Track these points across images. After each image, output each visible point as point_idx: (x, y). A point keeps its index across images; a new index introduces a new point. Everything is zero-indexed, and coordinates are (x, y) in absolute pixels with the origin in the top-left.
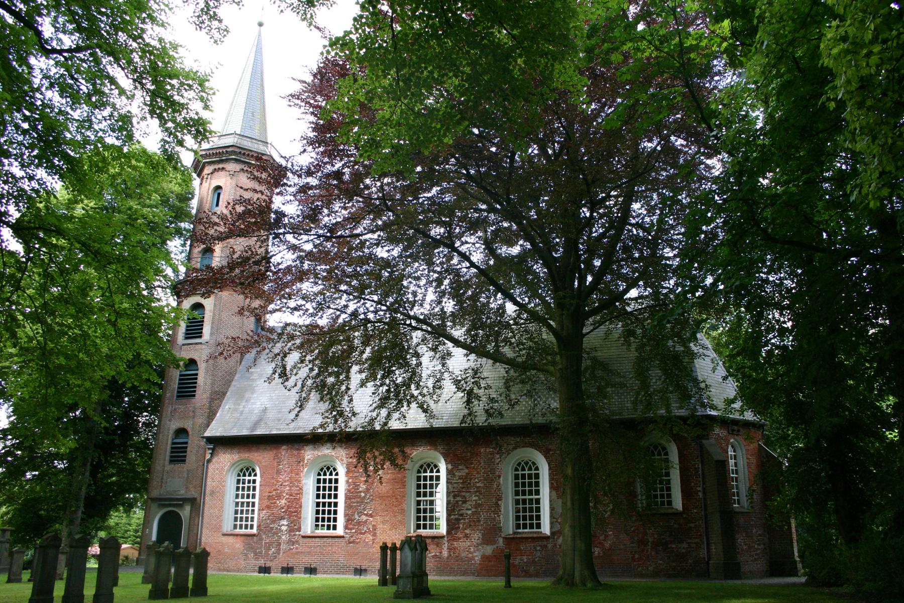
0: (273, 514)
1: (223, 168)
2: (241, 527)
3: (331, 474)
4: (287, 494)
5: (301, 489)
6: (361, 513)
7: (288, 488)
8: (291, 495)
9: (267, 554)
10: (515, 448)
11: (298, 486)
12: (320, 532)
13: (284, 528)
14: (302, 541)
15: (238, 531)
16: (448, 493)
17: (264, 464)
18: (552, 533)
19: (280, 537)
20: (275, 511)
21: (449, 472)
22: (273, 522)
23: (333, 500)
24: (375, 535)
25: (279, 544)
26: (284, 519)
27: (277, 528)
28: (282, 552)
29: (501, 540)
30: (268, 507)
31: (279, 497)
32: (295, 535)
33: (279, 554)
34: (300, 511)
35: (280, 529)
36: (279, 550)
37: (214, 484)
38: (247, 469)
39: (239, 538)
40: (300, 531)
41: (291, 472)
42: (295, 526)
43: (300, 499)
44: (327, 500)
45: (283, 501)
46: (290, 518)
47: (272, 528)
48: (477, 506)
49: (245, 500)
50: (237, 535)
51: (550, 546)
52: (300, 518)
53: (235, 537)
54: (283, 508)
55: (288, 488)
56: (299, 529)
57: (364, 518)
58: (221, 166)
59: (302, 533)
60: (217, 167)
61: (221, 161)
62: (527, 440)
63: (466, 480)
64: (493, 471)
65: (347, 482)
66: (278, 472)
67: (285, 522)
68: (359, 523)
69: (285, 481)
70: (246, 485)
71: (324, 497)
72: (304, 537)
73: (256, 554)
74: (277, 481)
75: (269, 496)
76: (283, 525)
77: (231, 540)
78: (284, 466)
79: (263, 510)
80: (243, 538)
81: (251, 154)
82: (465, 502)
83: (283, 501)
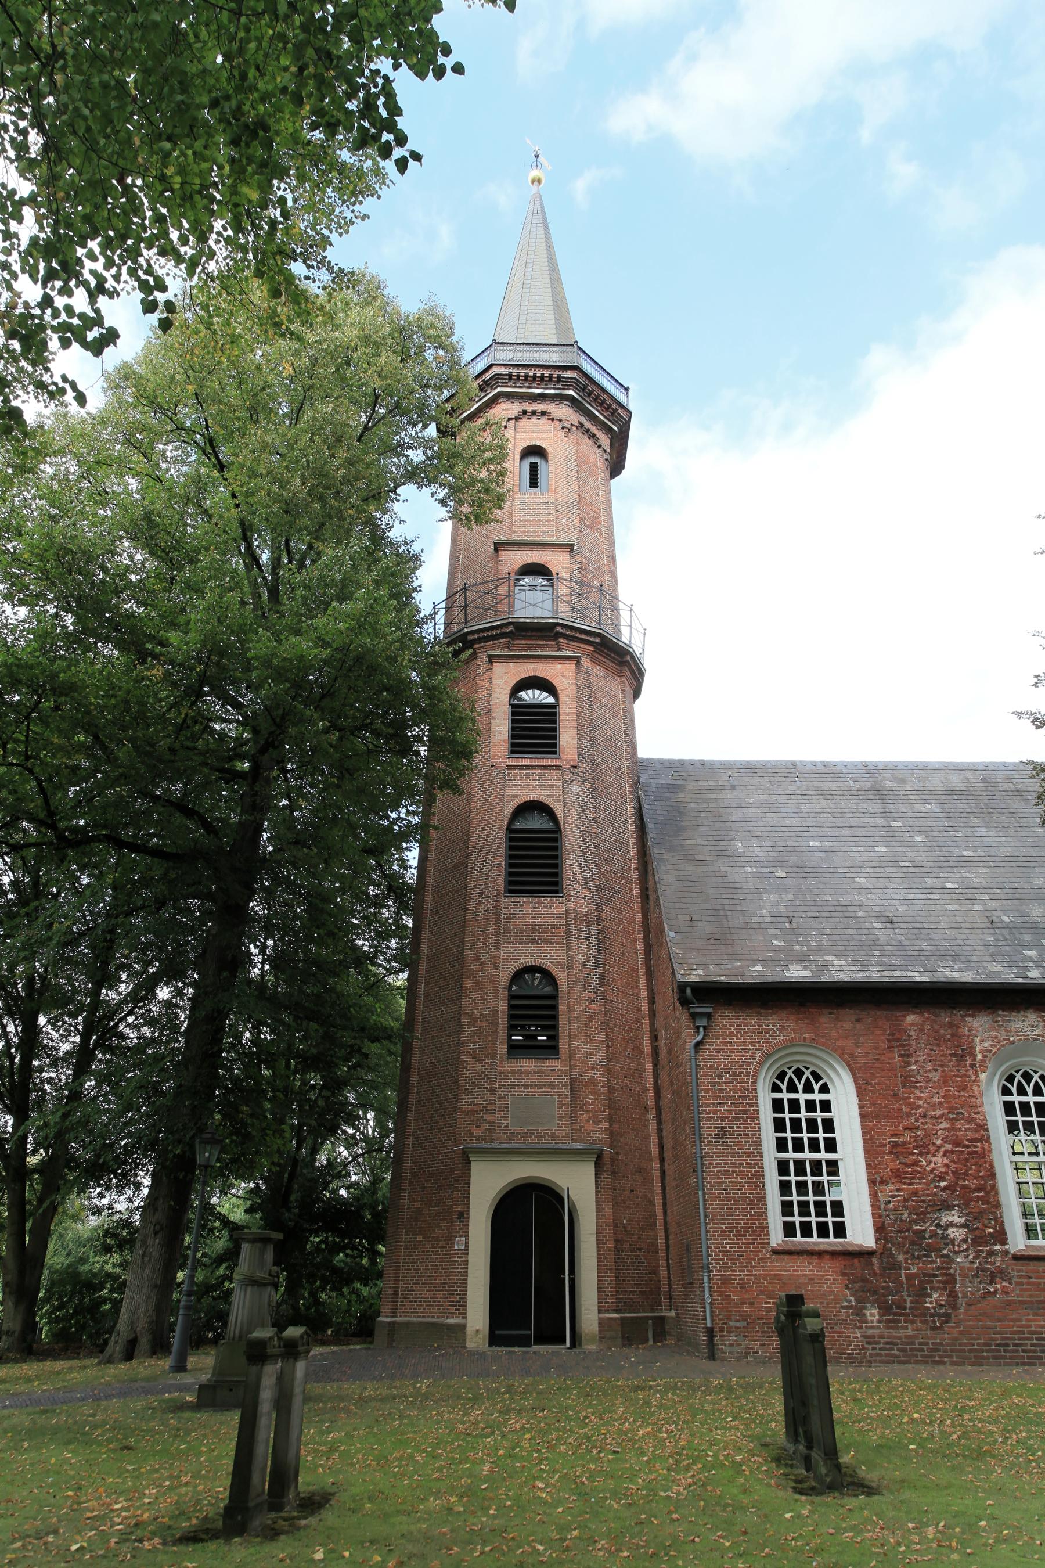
0: (915, 1193)
1: (544, 413)
4: (945, 1140)
7: (944, 1125)
8: (957, 1144)
9: (920, 1313)
11: (970, 1120)
13: (956, 1234)
14: (1015, 1271)
17: (863, 1060)
19: (948, 1260)
20: (918, 1185)
22: (922, 1216)
23: (823, 1155)
25: (951, 1280)
26: (950, 1208)
27: (934, 1235)
28: (961, 1301)
30: (898, 1175)
32: (992, 1253)
33: (955, 1307)
34: (994, 1187)
35: (945, 1237)
36: (953, 1295)
37: (723, 1110)
39: (828, 1266)
40: (1004, 1242)
41: (945, 1080)
44: (807, 1155)
46: (967, 1205)
47: (920, 1234)
49: (807, 1155)
50: (820, 1254)
52: (998, 1205)
53: (815, 1261)
54: (942, 1179)
55: (944, 1125)
56: (1001, 1237)
58: (539, 407)
60: (529, 407)
66: (908, 1082)
67: (954, 1217)
69: (934, 1107)
70: (803, 1115)
72: (1017, 1258)
73: (885, 1309)
74: (912, 1106)
75: (895, 1145)
76: (952, 1224)
78: (921, 1063)
79: (883, 1182)
80: (838, 1264)
83: (939, 1160)
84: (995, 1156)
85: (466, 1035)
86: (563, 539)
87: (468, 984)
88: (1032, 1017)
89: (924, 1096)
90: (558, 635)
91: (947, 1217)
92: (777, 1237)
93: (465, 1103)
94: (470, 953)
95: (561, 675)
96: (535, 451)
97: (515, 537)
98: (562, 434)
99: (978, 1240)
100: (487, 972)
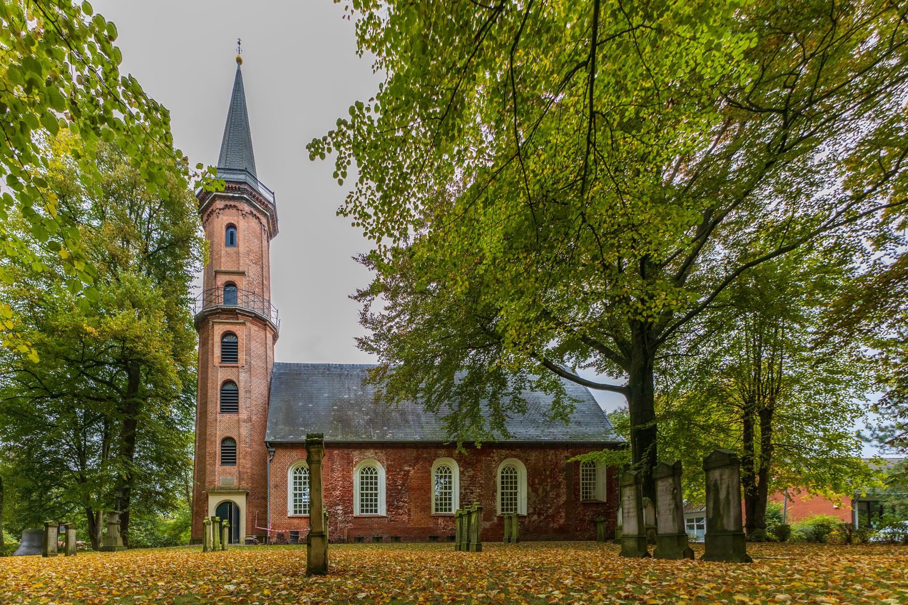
1: (235, 206)
2: (300, 512)
3: (371, 473)
5: (352, 483)
6: (398, 501)
10: (505, 458)
12: (365, 514)
15: (298, 514)
16: (461, 487)
18: (529, 514)
21: (461, 473)
24: (409, 515)
29: (495, 518)
31: (334, 489)
38: (302, 469)
42: (348, 510)
43: (351, 490)
45: (338, 492)
48: (480, 496)
51: (526, 522)
56: (352, 512)
57: (401, 504)
58: (233, 203)
59: (355, 515)
60: (229, 203)
61: (233, 198)
62: (513, 453)
63: (473, 478)
64: (491, 473)
65: (387, 478)
66: (332, 471)
67: (340, 507)
68: (398, 508)
70: (303, 480)
71: (367, 490)
77: (296, 521)
81: (260, 198)
82: (472, 493)
83: (338, 492)
84: (354, 491)
85: (208, 459)
86: (241, 269)
87: (208, 443)
88: (372, 451)
89: (336, 474)
90: (237, 313)
91: (338, 507)
92: (291, 513)
93: (207, 479)
94: (208, 433)
95: (240, 332)
96: (231, 226)
97: (223, 269)
98: (241, 217)
99: (345, 513)
100: (213, 439)
